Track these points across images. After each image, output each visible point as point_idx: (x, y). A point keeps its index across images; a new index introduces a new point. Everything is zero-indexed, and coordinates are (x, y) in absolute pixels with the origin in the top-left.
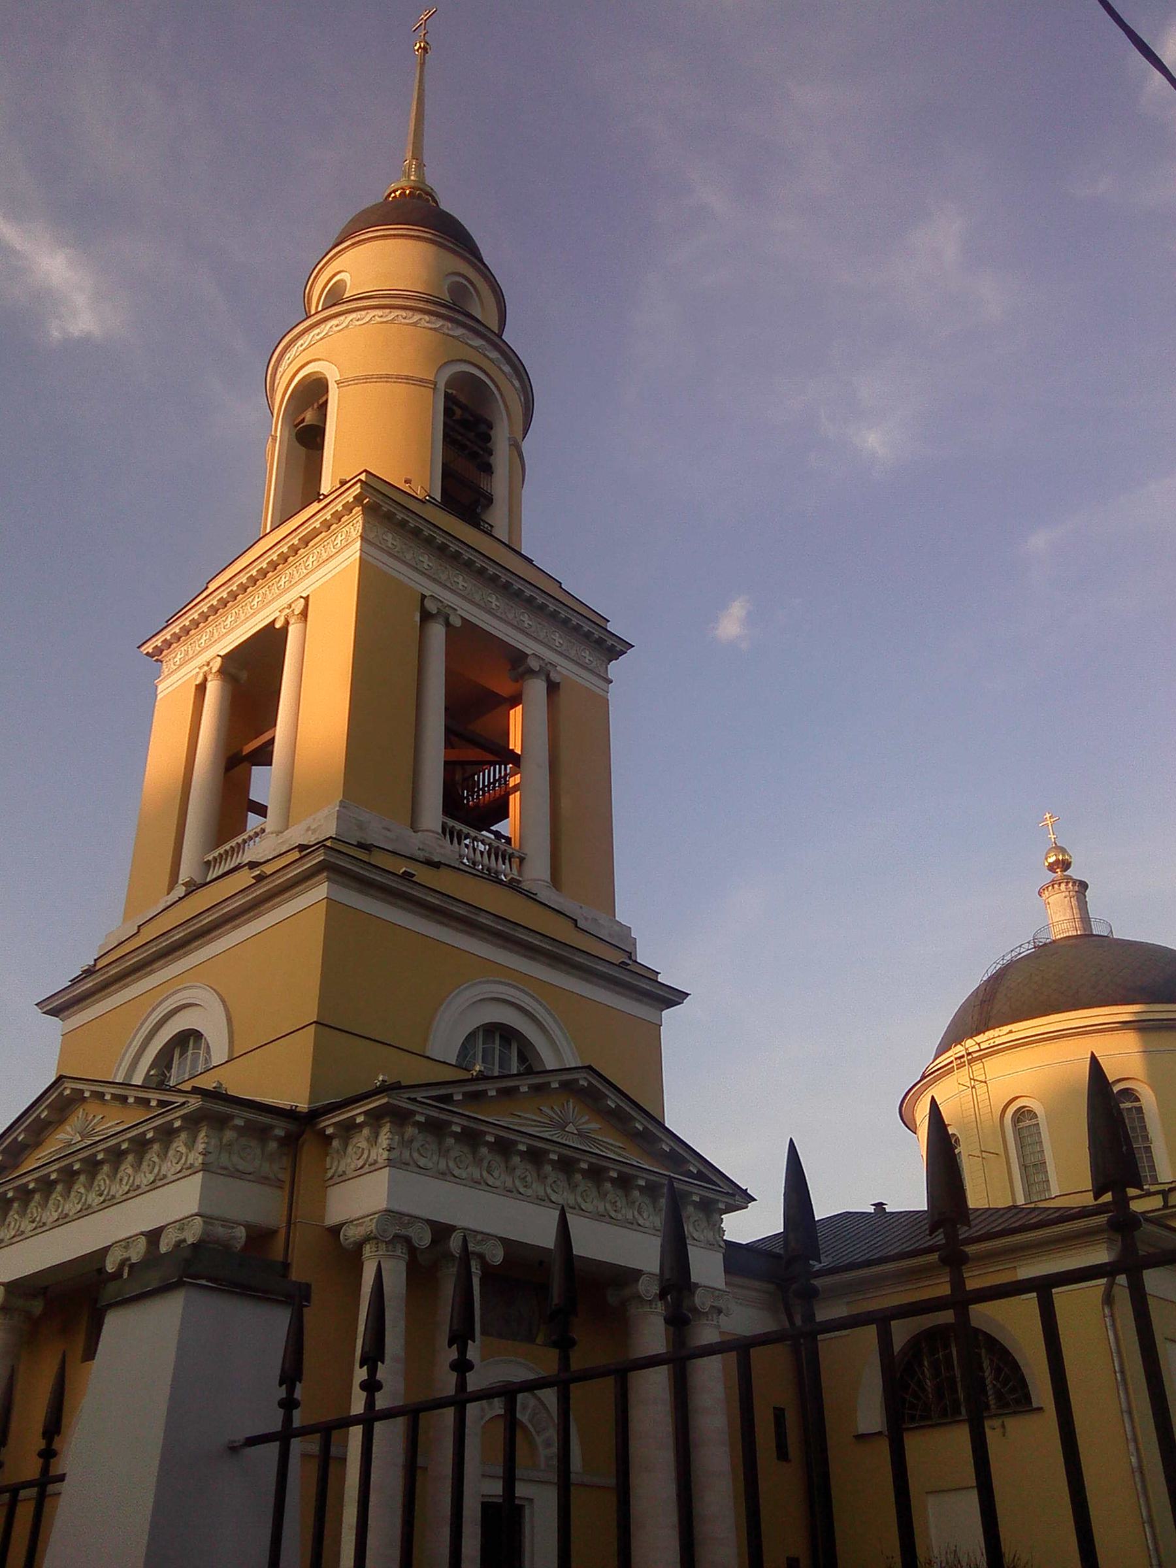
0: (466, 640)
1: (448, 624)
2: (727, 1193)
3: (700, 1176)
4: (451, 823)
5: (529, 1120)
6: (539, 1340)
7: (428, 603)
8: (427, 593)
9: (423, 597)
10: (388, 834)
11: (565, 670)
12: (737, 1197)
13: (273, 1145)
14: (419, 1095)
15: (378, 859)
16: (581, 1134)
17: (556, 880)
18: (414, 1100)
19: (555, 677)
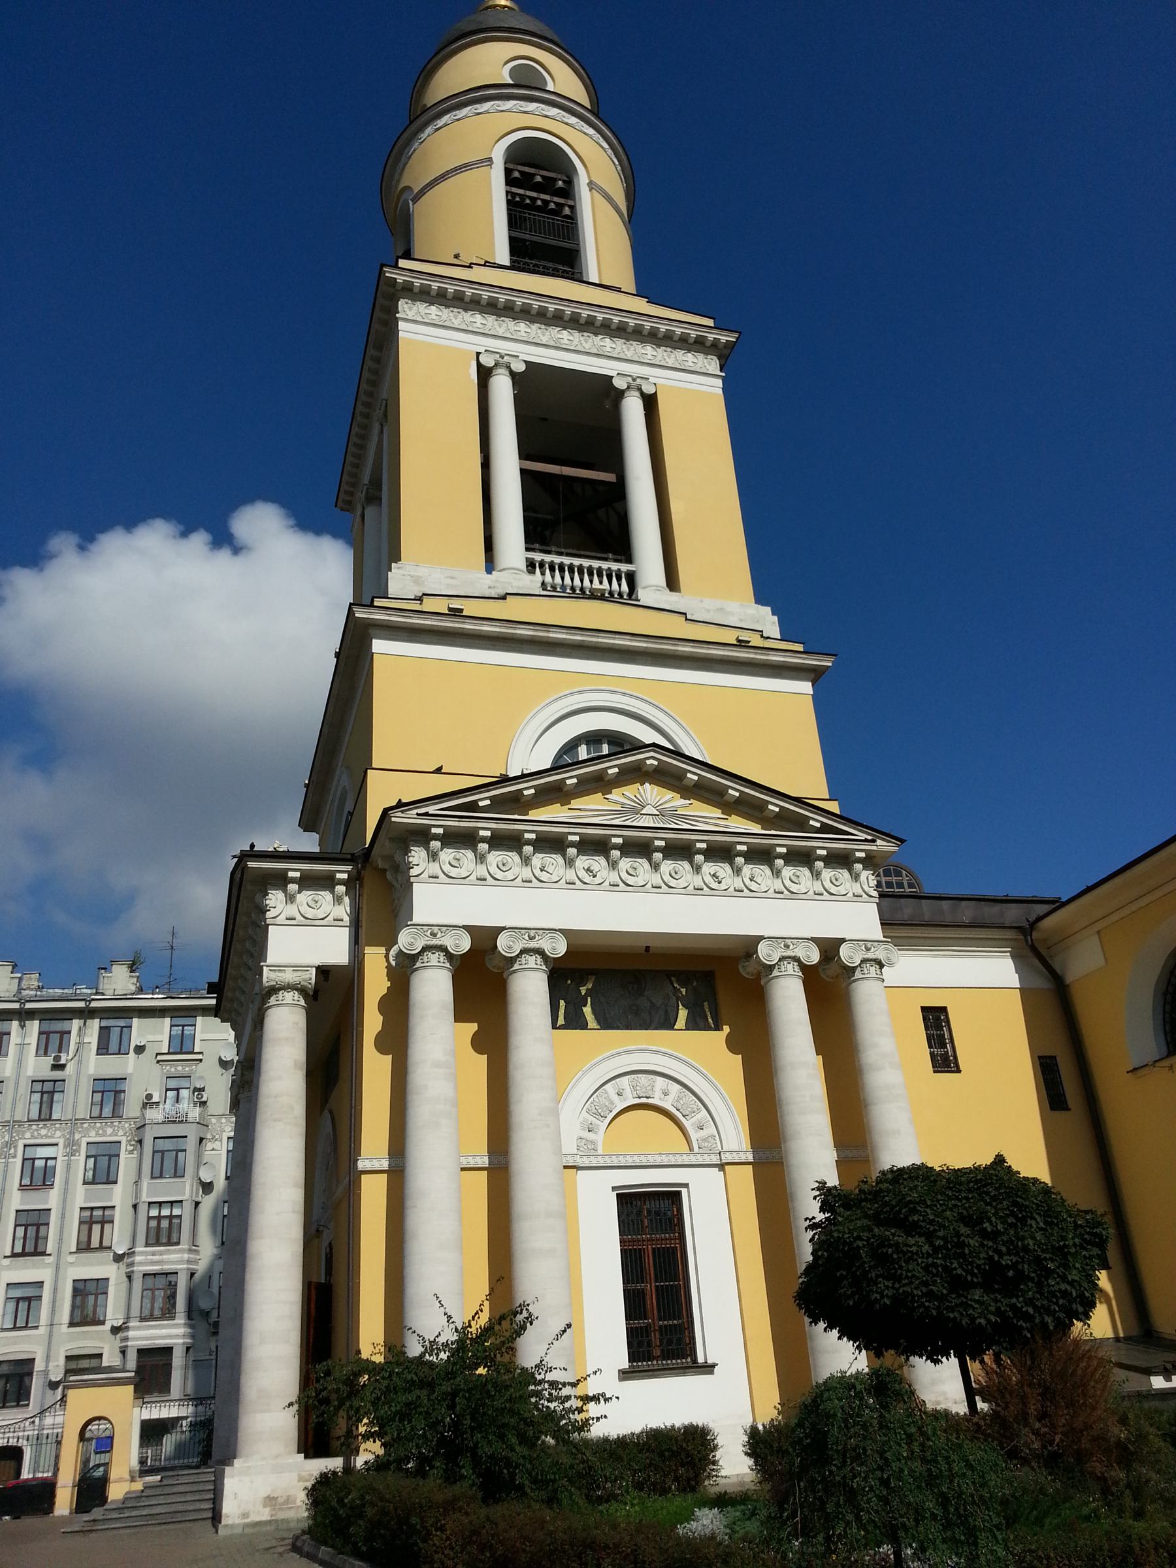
0: (534, 384)
1: (513, 374)
2: (866, 840)
3: (825, 828)
4: (538, 557)
5: (591, 809)
6: (681, 1022)
7: (482, 359)
8: (482, 350)
9: (478, 354)
10: (453, 582)
11: (659, 380)
12: (879, 842)
13: (340, 889)
14: (431, 809)
15: (429, 605)
16: (662, 814)
17: (672, 582)
18: (426, 814)
19: (649, 389)
